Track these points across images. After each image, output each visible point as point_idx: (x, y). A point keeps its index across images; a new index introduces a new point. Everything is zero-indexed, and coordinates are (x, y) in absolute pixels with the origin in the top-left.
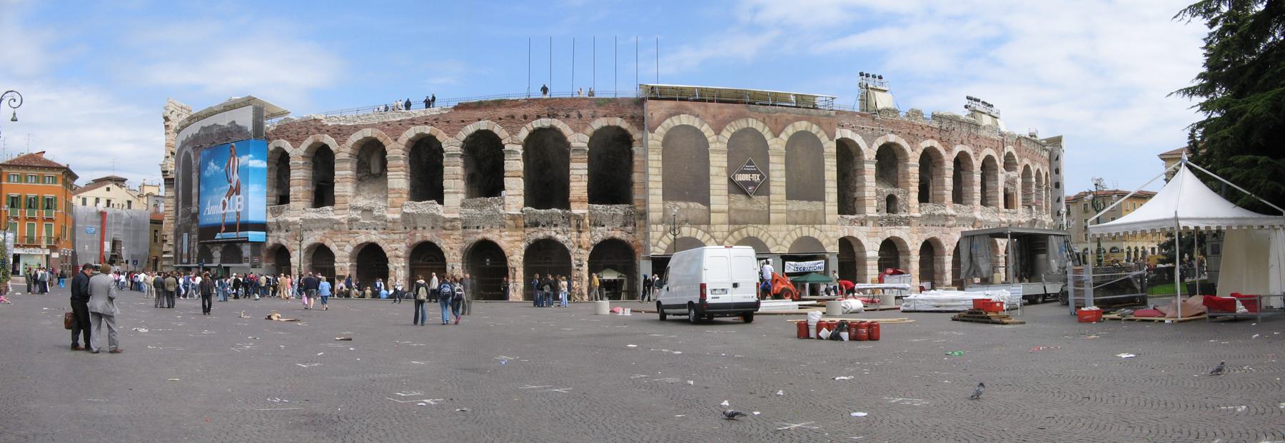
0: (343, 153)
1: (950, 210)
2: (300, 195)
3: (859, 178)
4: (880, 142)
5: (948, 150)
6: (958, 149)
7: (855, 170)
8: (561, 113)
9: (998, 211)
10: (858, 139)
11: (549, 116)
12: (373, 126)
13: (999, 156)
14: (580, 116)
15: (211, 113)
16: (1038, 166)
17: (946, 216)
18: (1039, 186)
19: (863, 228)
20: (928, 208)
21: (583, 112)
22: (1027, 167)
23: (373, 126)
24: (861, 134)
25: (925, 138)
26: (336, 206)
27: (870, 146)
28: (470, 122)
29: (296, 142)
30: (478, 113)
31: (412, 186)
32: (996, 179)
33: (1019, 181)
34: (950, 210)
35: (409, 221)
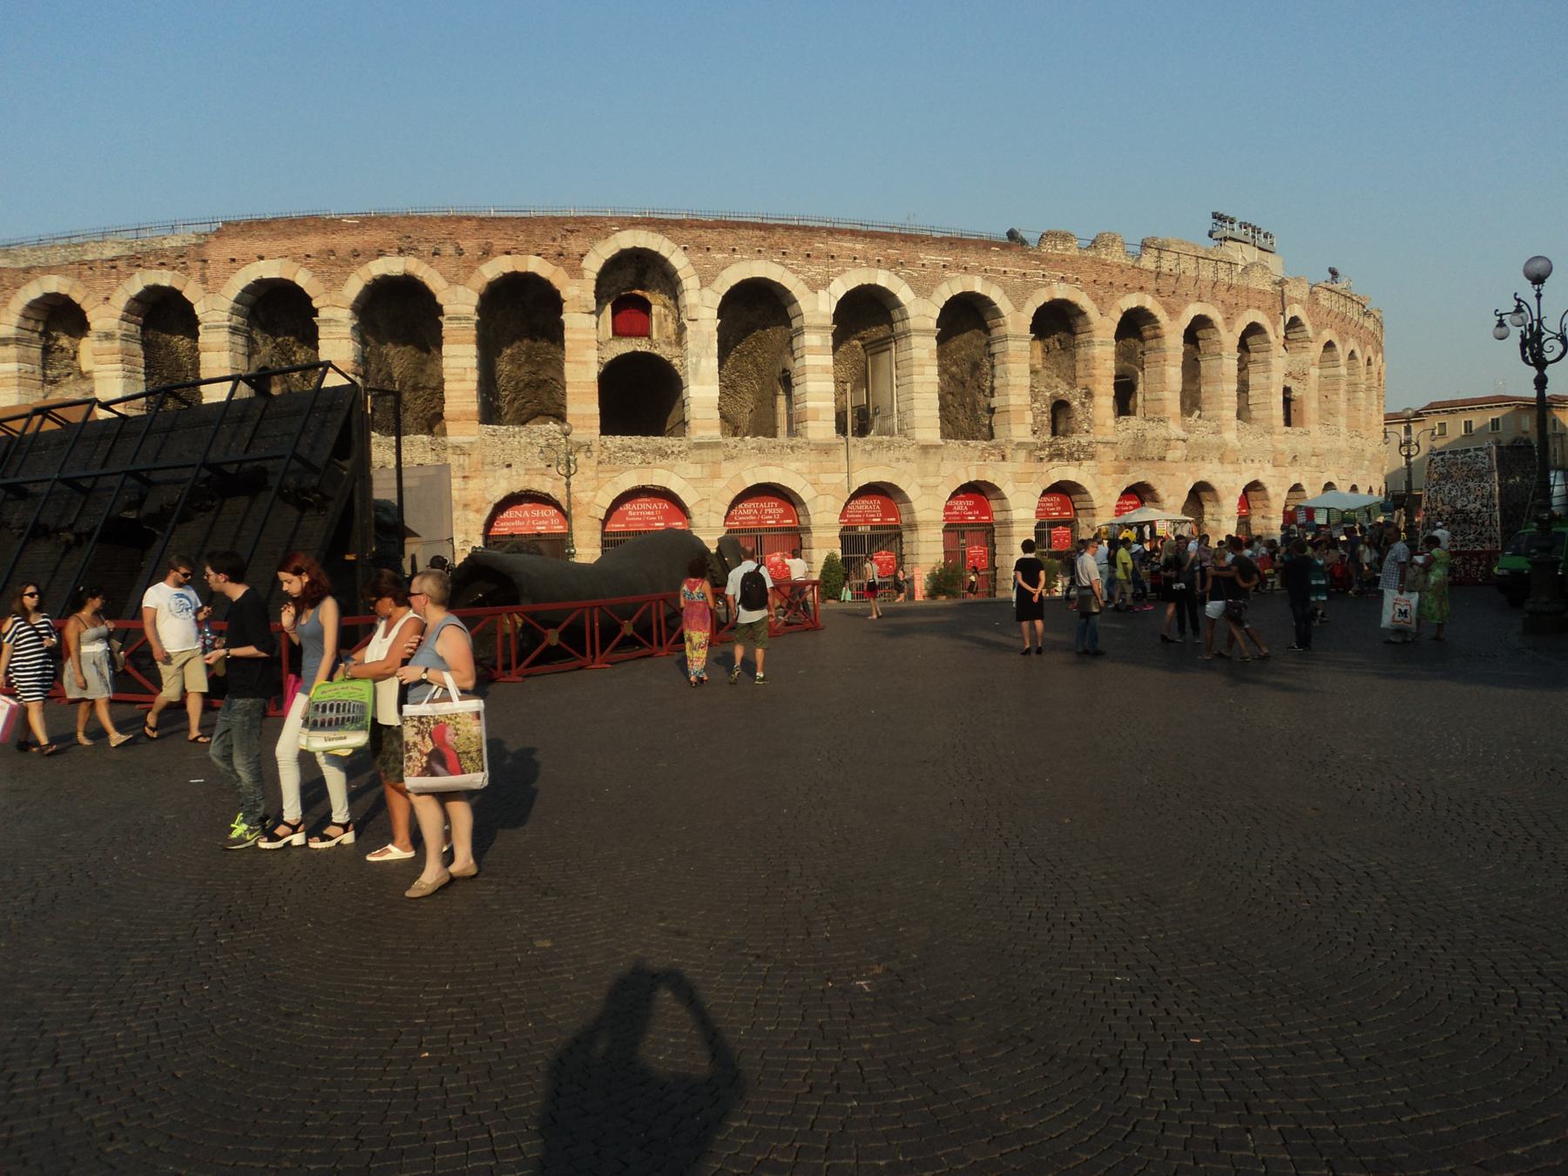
1: (1175, 429)
4: (1041, 298)
5: (1173, 313)
6: (1192, 310)
8: (425, 248)
9: (1270, 431)
10: (995, 294)
11: (401, 251)
13: (1275, 323)
14: (460, 252)
16: (1352, 345)
19: (1007, 466)
21: (468, 245)
24: (1003, 286)
25: (1130, 290)
27: (1019, 307)
28: (246, 262)
30: (259, 246)
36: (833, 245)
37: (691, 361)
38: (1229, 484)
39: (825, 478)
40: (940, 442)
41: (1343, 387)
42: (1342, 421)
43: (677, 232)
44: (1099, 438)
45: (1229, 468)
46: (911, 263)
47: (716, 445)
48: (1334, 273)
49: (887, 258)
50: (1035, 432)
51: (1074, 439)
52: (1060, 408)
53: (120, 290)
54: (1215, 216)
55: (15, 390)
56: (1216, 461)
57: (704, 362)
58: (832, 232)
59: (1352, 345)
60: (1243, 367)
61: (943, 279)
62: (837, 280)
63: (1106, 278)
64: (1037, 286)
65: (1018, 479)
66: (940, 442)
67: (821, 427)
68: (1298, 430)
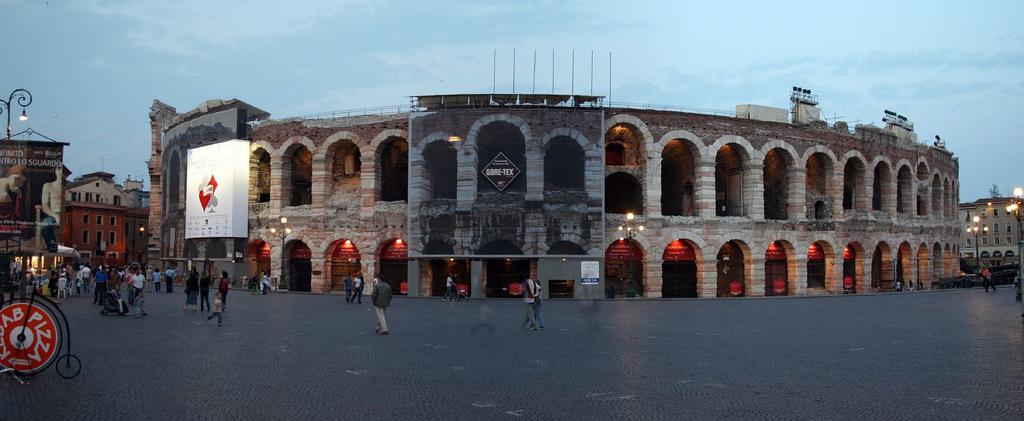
0: (319, 153)
2: (279, 194)
3: (791, 186)
4: (811, 151)
5: (869, 159)
6: (878, 159)
7: (788, 178)
9: (911, 218)
10: (791, 149)
12: (348, 129)
13: (914, 166)
15: (197, 114)
17: (867, 221)
18: (946, 195)
19: (794, 233)
20: (852, 214)
22: (937, 176)
23: (348, 129)
24: (794, 145)
26: (313, 205)
29: (276, 142)
31: (382, 186)
32: (910, 185)
33: (930, 189)
34: (871, 217)
35: (378, 222)
36: (715, 124)
37: (648, 178)
38: (894, 241)
39: (711, 237)
40: (765, 221)
41: (942, 196)
42: (942, 212)
43: (644, 116)
44: (837, 220)
45: (893, 235)
46: (753, 133)
47: (660, 219)
48: (937, 137)
49: (741, 130)
50: (807, 216)
51: (824, 221)
52: (819, 205)
53: (376, 138)
54: (886, 112)
55: (323, 184)
56: (889, 235)
57: (655, 179)
58: (716, 118)
59: (946, 175)
60: (899, 187)
61: (767, 141)
62: (717, 140)
63: (840, 143)
64: (809, 146)
65: (802, 239)
66: (765, 221)
67: (709, 213)
68: (923, 217)
